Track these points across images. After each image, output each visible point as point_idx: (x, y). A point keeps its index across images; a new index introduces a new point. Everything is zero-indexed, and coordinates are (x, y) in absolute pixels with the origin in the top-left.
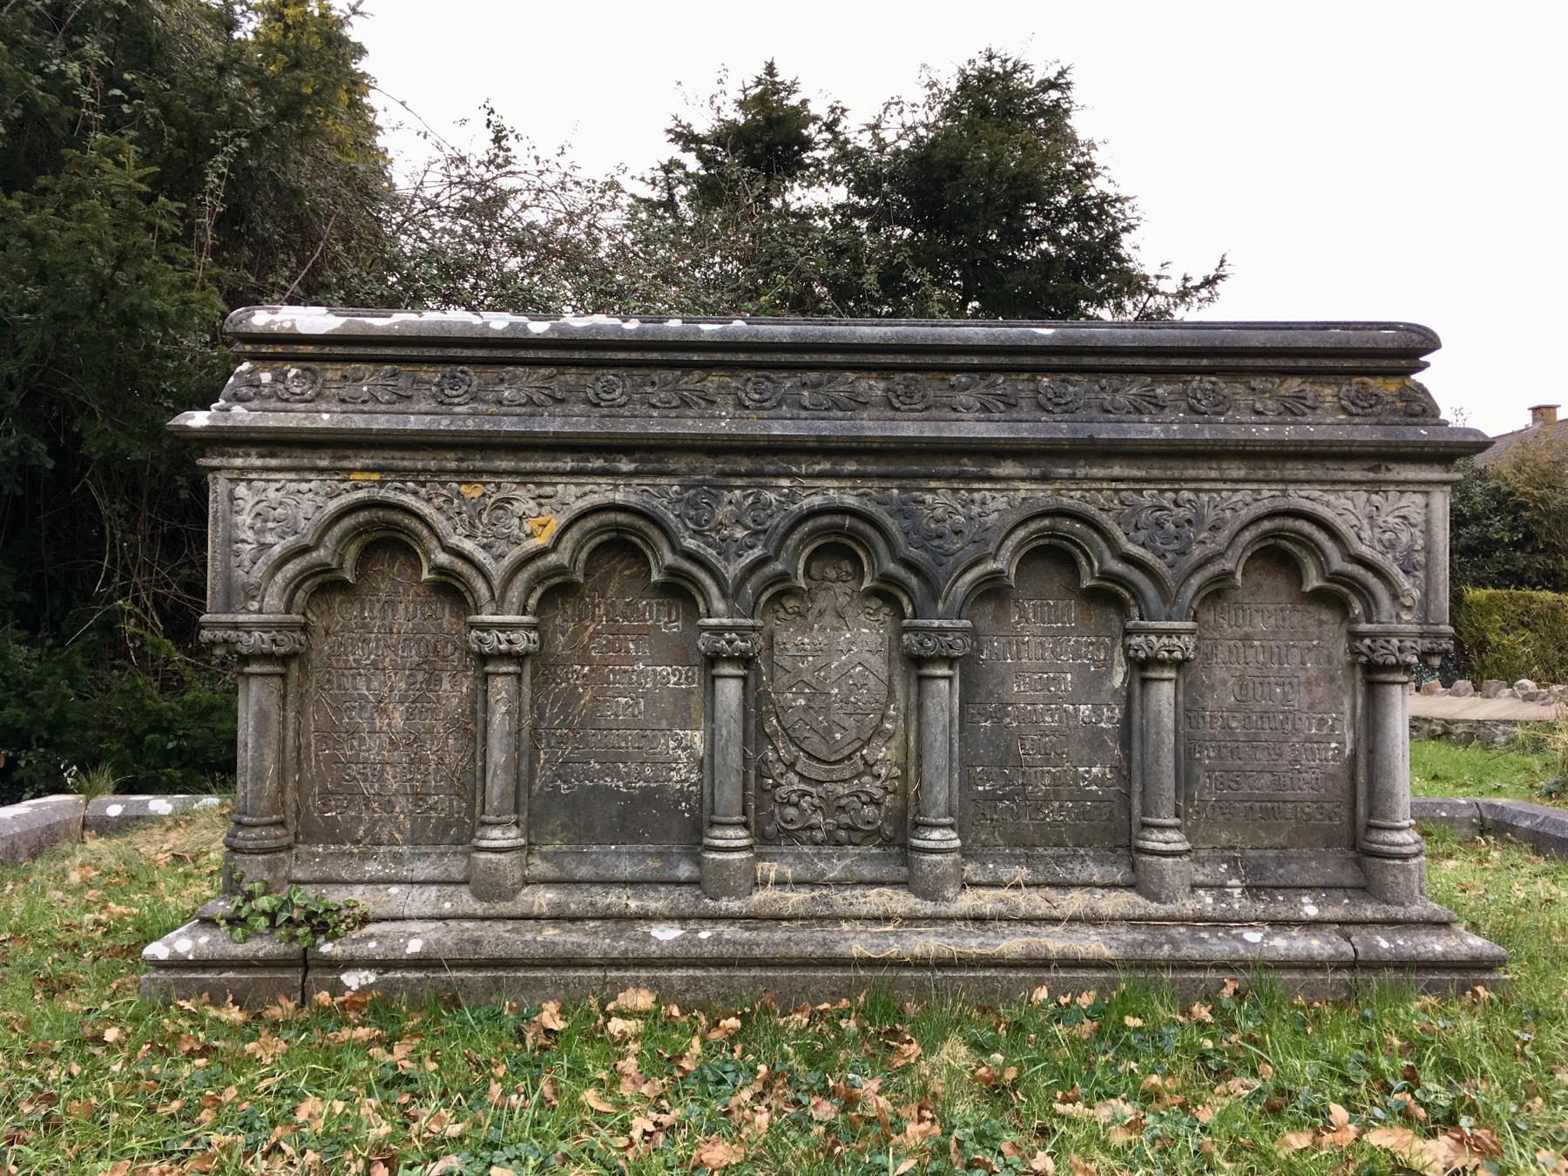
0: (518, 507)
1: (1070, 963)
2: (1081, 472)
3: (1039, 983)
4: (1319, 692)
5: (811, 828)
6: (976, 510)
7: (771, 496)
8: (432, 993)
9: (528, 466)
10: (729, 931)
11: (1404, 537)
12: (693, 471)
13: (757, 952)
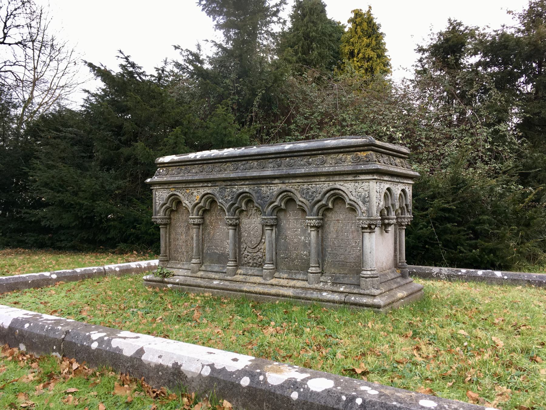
0: (194, 194)
1: (284, 296)
2: (290, 181)
3: (278, 299)
4: (355, 234)
5: (249, 263)
6: (271, 191)
7: (234, 190)
8: (183, 289)
9: (195, 186)
10: (227, 283)
11: (363, 194)
12: (221, 185)
13: (228, 287)
